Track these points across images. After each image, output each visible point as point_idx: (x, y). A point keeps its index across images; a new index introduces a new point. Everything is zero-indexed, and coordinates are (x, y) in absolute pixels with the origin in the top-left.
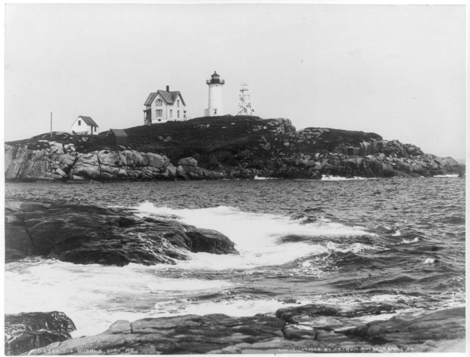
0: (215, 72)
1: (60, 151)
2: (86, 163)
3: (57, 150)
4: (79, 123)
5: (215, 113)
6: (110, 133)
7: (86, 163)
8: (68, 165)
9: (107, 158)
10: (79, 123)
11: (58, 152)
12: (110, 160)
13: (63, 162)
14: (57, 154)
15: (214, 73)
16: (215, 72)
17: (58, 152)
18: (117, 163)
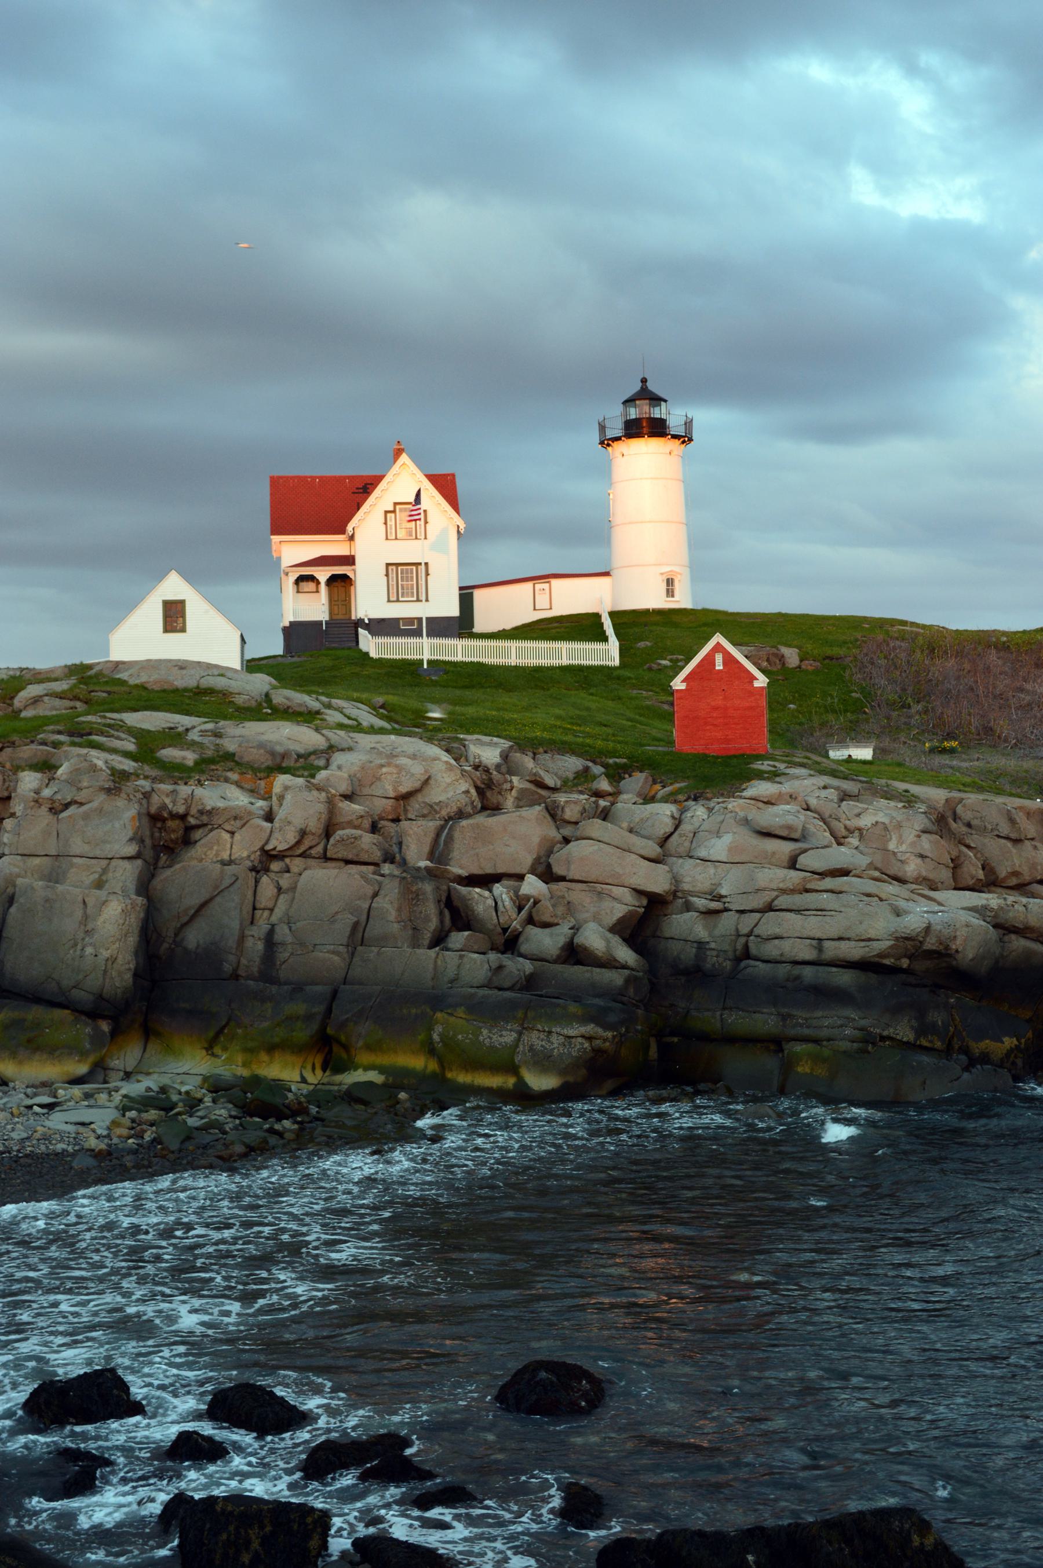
0: (644, 381)
1: (451, 788)
2: (844, 872)
3: (426, 782)
4: (174, 616)
5: (670, 593)
6: (709, 659)
7: (844, 872)
8: (639, 892)
9: (910, 835)
10: (174, 616)
11: (436, 795)
12: (926, 844)
13: (558, 870)
14: (432, 810)
15: (637, 386)
16: (644, 381)
17: (436, 795)
18: (956, 865)
